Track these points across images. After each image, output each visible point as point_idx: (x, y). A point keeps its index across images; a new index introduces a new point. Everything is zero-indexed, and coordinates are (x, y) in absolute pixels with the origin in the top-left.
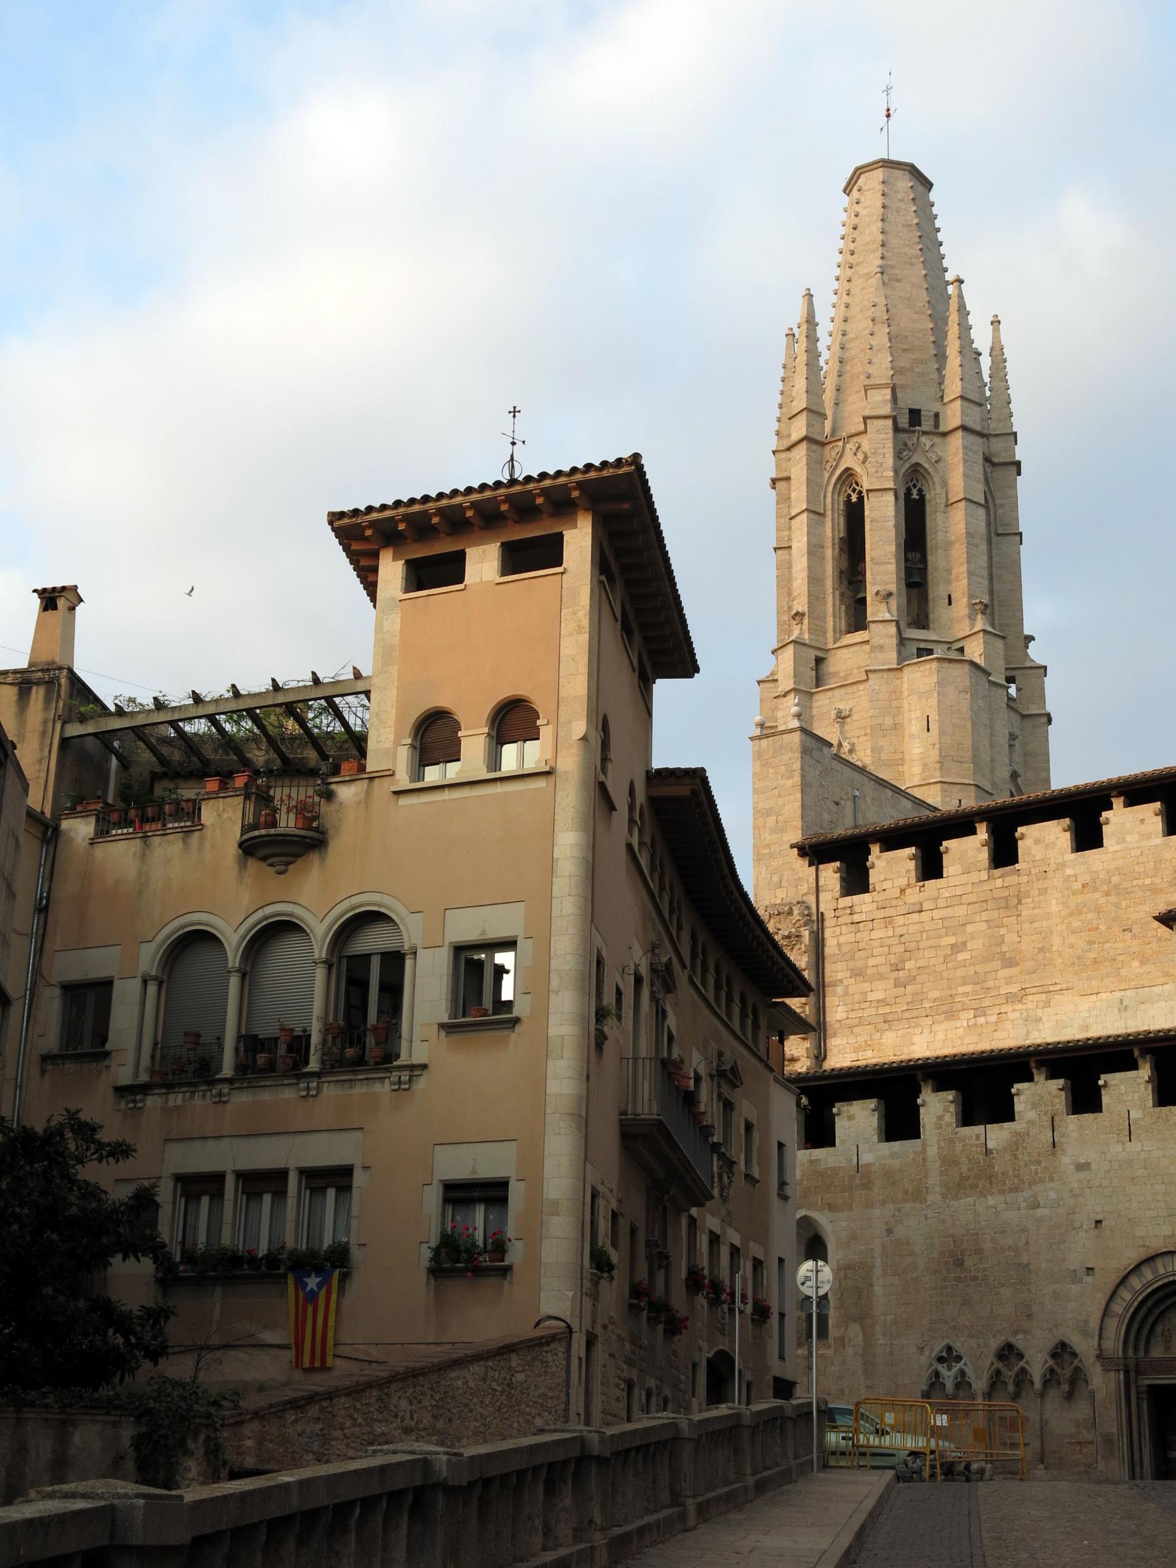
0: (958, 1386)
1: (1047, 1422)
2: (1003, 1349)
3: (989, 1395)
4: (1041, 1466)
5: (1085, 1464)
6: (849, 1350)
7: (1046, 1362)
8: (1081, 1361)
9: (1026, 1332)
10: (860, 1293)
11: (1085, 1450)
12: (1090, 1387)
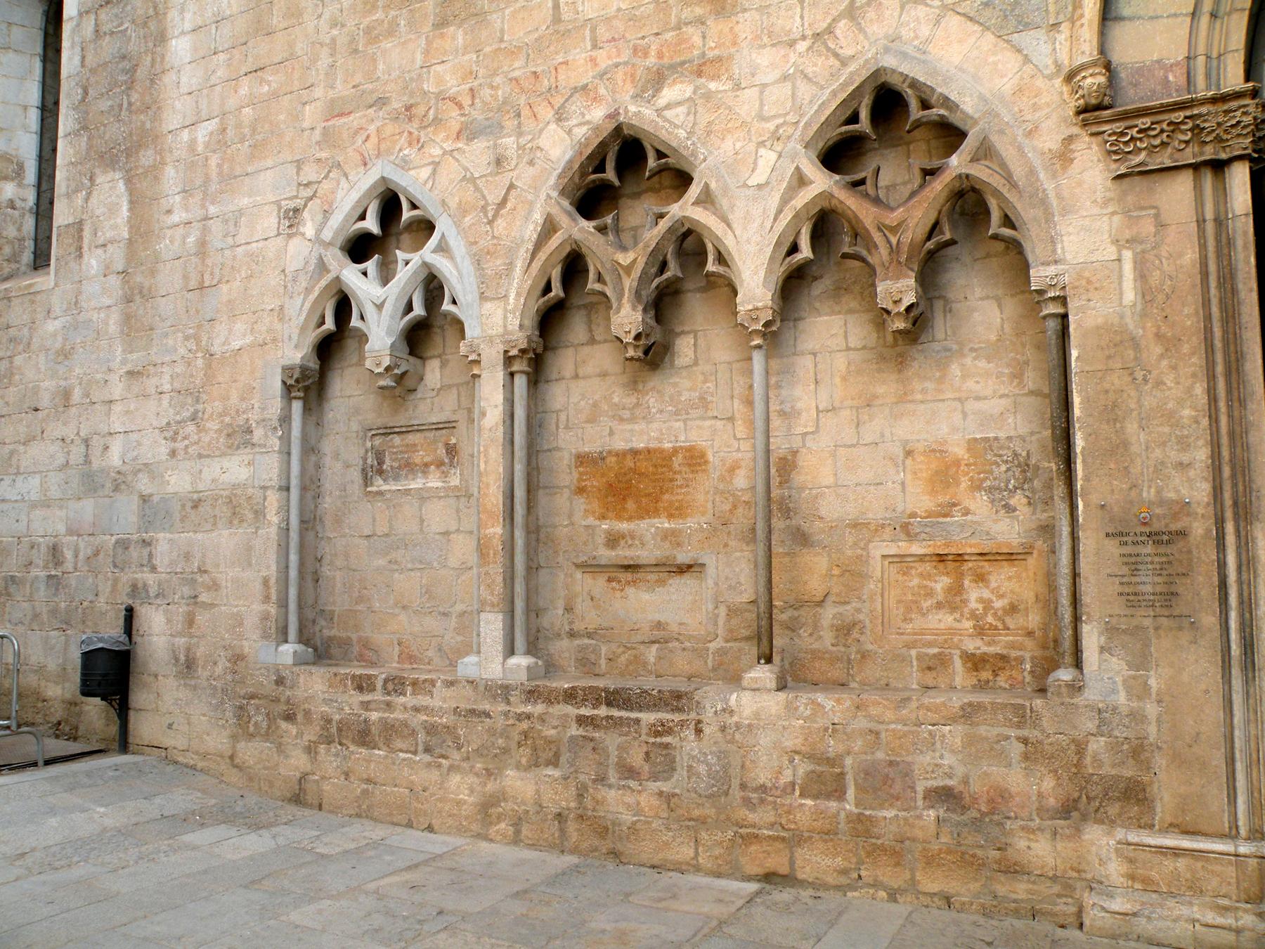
0: (417, 337)
1: (787, 465)
2: (596, 161)
3: (536, 360)
4: (763, 674)
5: (975, 662)
6: (93, 262)
7: (801, 180)
8: (985, 152)
9: (702, 68)
10: (134, 68)
11: (974, 595)
12: (1039, 275)
